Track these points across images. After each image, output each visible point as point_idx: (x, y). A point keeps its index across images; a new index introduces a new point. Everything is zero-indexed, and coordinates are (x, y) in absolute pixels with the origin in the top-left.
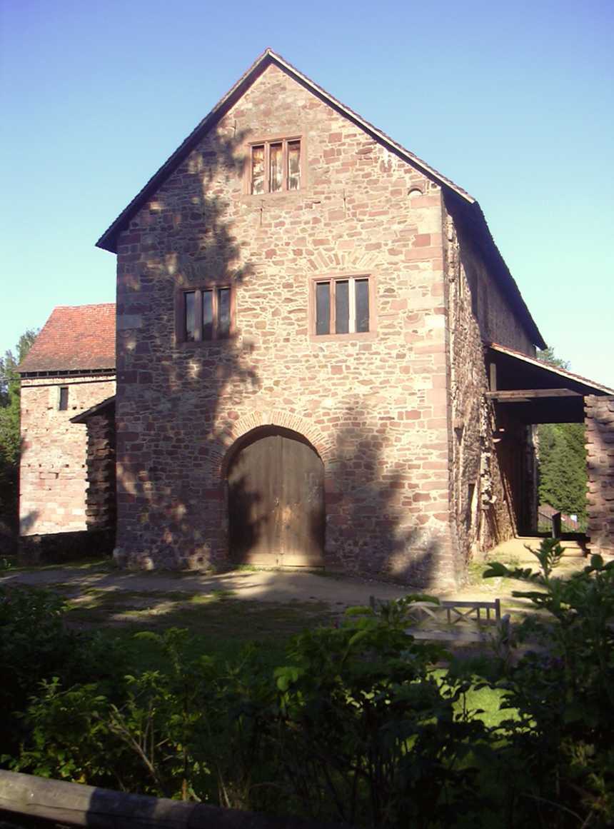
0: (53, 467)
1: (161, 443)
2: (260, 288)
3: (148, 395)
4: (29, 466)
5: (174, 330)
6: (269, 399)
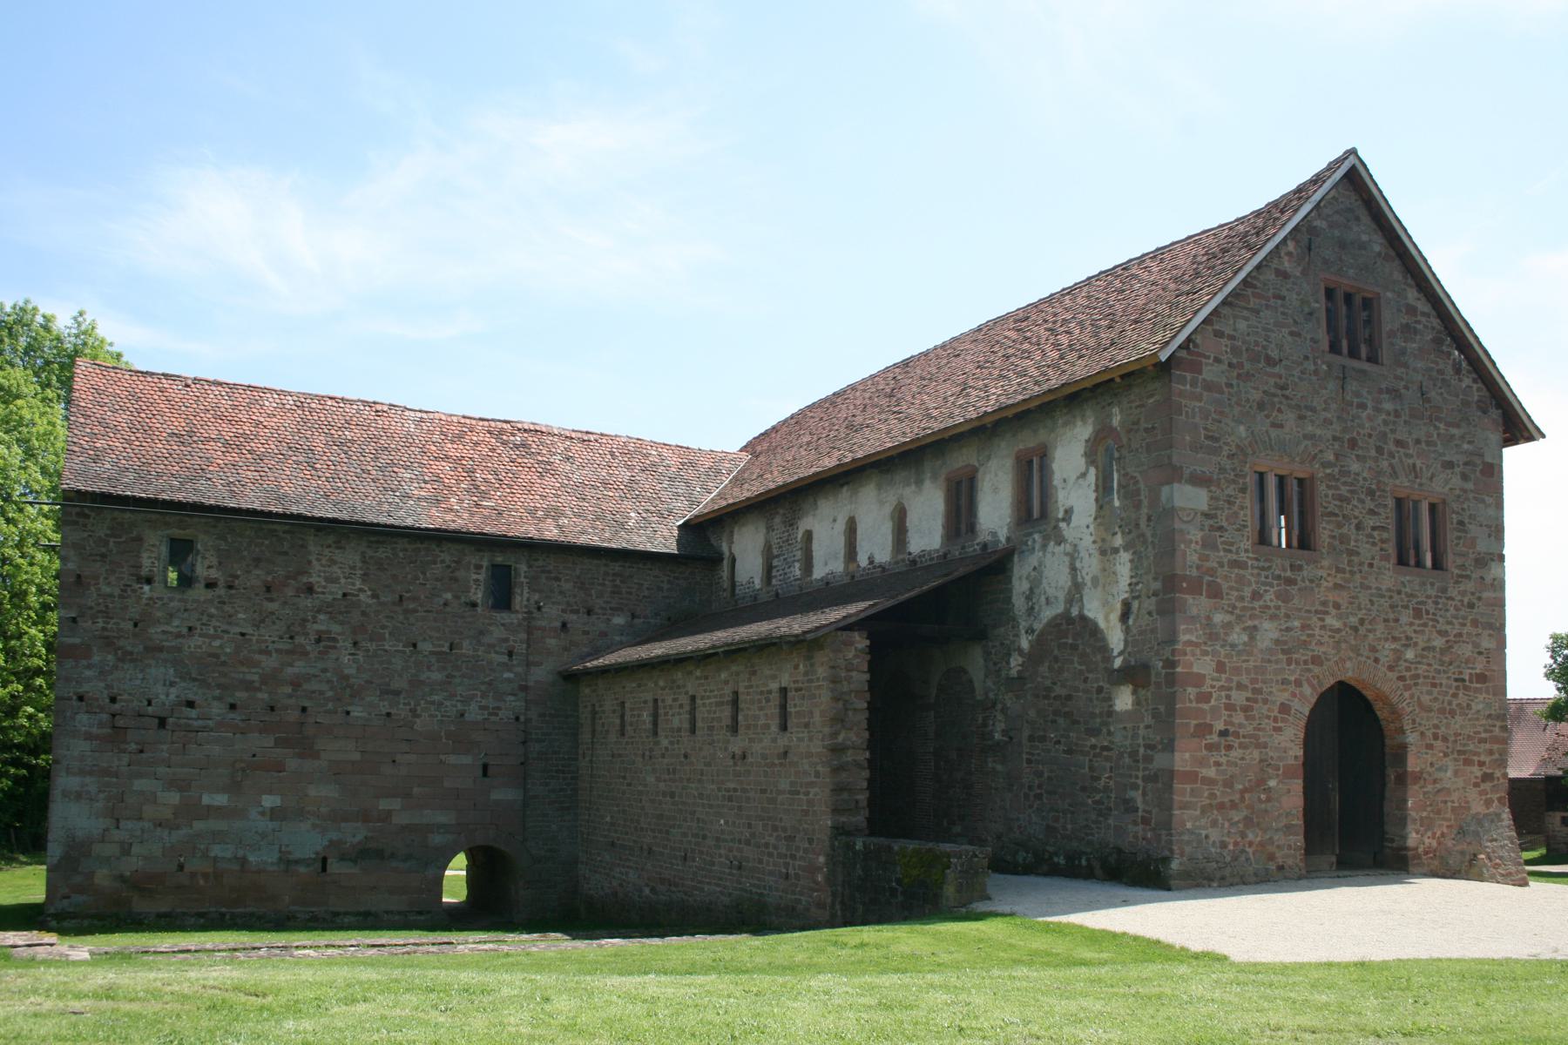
0: (150, 704)
1: (1234, 693)
2: (1343, 488)
3: (1218, 618)
4: (81, 698)
5: (1249, 524)
6: (1353, 642)
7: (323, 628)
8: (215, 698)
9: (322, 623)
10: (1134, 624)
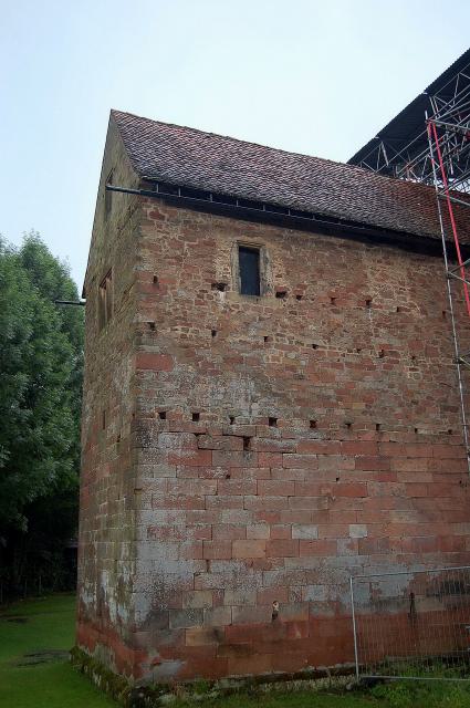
4: (163, 415)
7: (384, 342)
8: (296, 415)
9: (383, 338)
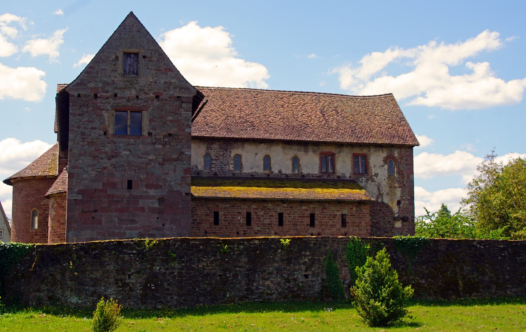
10: (402, 206)
